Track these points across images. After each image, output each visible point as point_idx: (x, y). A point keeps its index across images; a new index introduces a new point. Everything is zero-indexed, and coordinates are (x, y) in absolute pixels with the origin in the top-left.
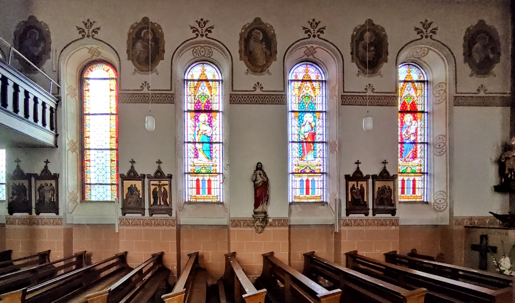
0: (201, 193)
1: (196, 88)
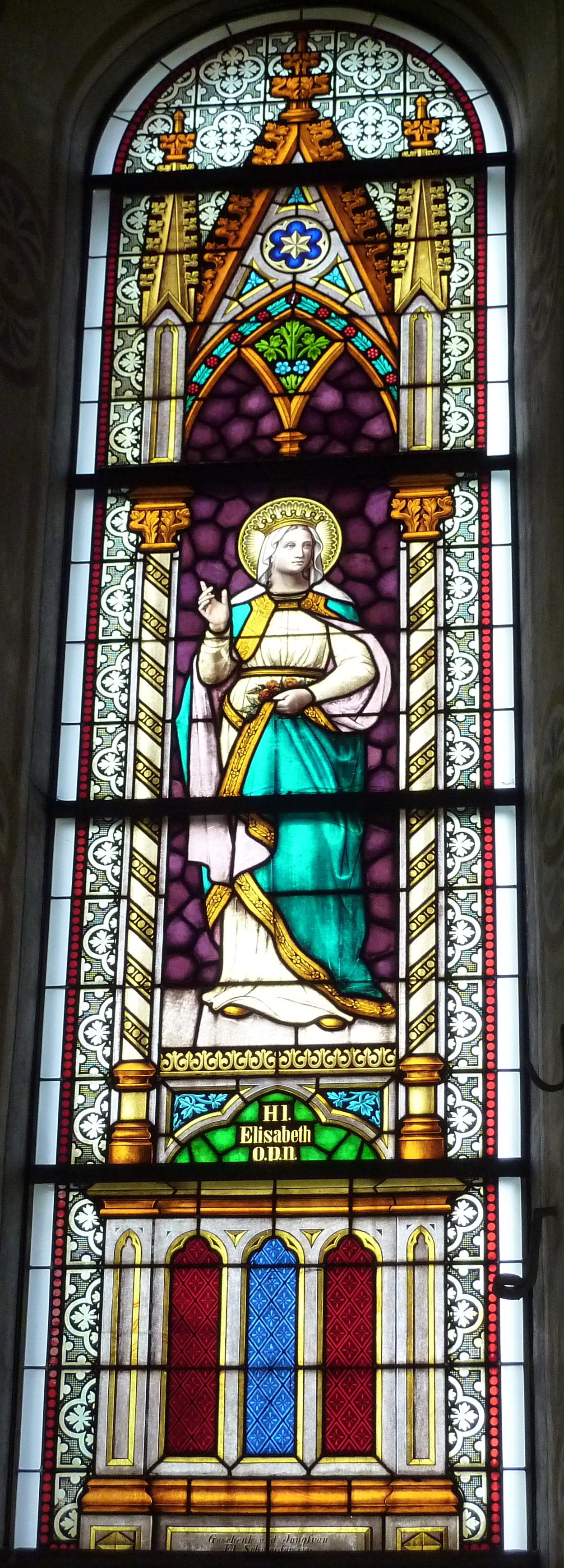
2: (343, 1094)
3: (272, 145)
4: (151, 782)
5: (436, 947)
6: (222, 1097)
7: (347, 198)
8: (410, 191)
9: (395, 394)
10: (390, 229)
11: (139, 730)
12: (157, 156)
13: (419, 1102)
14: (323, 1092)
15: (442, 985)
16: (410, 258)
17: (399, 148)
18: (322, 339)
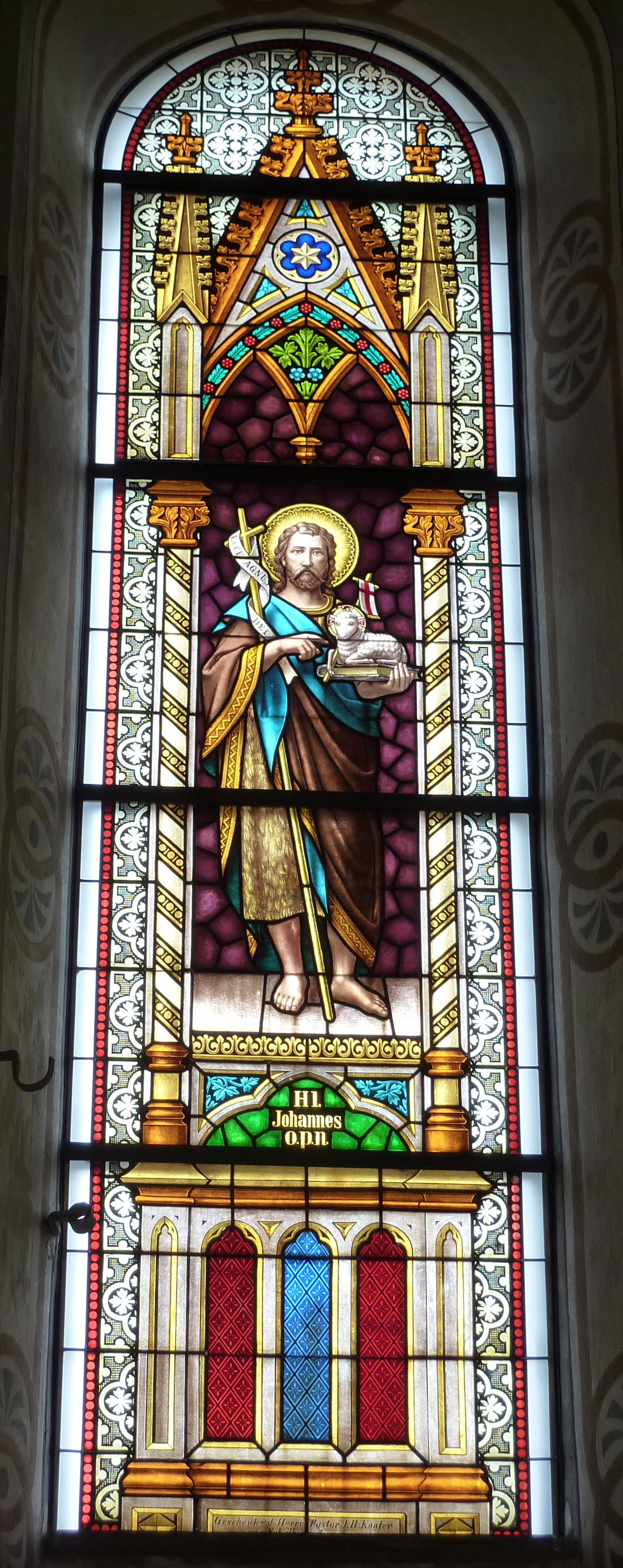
0: (266, 1424)
1: (219, 257)
2: (370, 1083)
5: (457, 945)
6: (254, 1082)
9: (406, 408)
10: (397, 249)
12: (166, 156)
13: (444, 1093)
14: (351, 1080)
15: (463, 982)
18: (335, 349)
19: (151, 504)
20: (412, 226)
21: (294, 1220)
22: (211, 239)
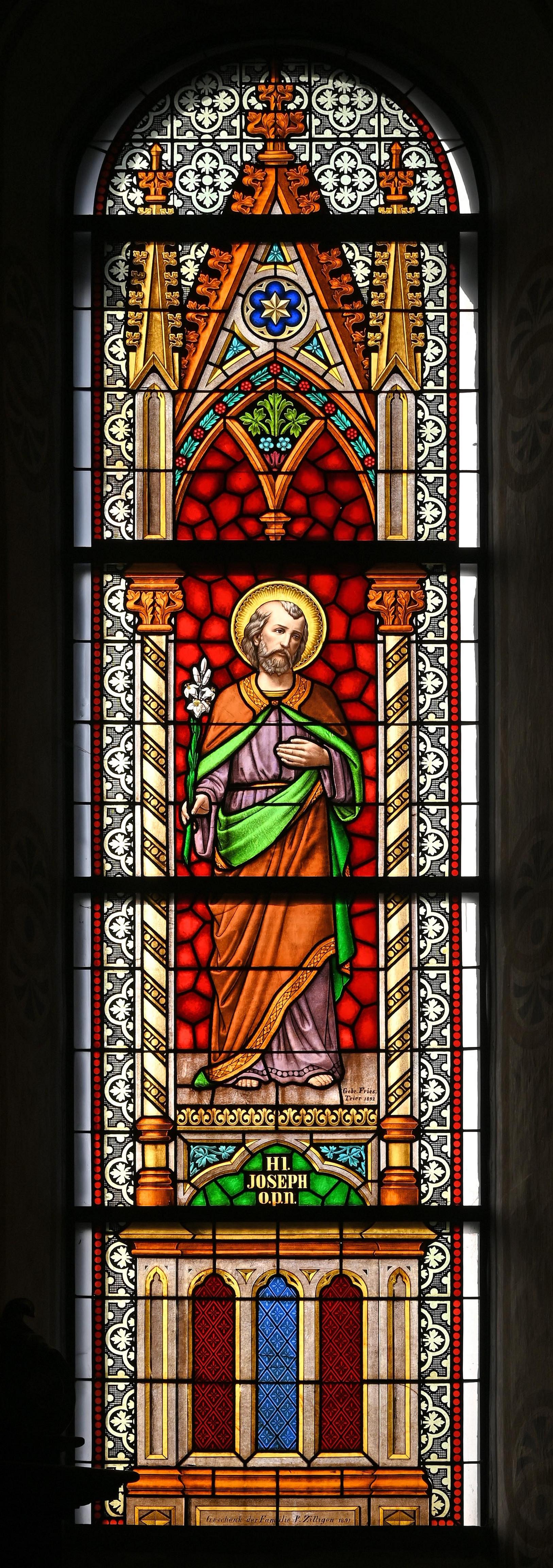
0: (243, 1441)
1: (189, 311)
2: (334, 1148)
3: (249, 191)
4: (158, 859)
7: (323, 258)
8: (386, 254)
10: (365, 297)
11: (144, 809)
16: (385, 329)
17: (374, 203)
19: (128, 587)
20: (382, 269)
21: (265, 1267)
22: (181, 293)
